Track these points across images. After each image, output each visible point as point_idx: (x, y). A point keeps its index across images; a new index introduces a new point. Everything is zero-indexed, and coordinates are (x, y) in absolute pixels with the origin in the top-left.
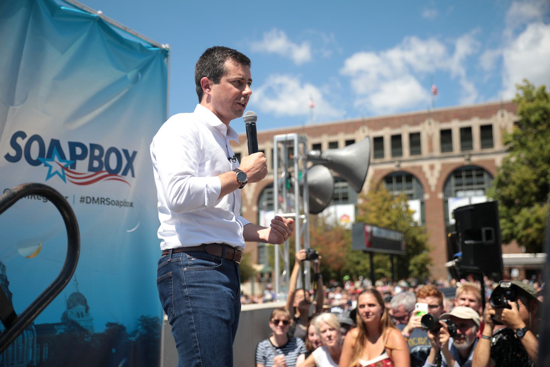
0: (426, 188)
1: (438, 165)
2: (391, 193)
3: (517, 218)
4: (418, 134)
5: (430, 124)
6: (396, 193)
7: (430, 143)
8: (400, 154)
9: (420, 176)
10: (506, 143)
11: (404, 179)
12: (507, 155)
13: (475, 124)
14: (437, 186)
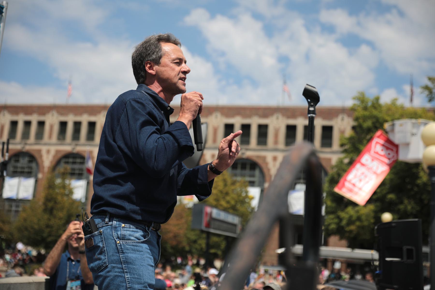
0: (267, 178)
1: (280, 156)
2: (235, 178)
3: (342, 215)
5: (277, 118)
6: (239, 179)
9: (263, 166)
10: (342, 145)
11: (248, 167)
12: (342, 156)
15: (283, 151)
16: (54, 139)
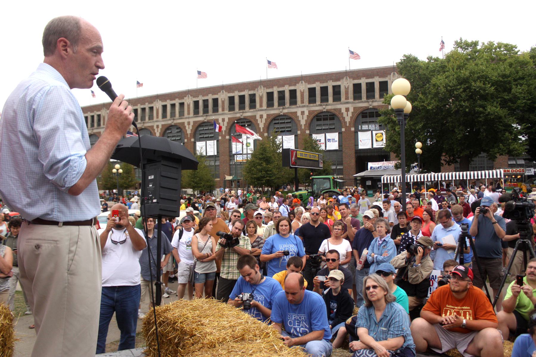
4: (339, 86)
7: (347, 93)
8: (327, 100)
13: (376, 80)
14: (350, 123)
15: (352, 103)
16: (192, 114)
